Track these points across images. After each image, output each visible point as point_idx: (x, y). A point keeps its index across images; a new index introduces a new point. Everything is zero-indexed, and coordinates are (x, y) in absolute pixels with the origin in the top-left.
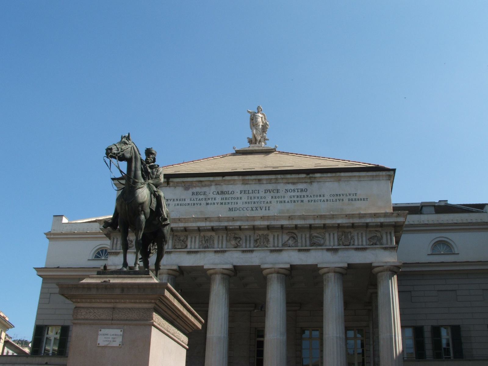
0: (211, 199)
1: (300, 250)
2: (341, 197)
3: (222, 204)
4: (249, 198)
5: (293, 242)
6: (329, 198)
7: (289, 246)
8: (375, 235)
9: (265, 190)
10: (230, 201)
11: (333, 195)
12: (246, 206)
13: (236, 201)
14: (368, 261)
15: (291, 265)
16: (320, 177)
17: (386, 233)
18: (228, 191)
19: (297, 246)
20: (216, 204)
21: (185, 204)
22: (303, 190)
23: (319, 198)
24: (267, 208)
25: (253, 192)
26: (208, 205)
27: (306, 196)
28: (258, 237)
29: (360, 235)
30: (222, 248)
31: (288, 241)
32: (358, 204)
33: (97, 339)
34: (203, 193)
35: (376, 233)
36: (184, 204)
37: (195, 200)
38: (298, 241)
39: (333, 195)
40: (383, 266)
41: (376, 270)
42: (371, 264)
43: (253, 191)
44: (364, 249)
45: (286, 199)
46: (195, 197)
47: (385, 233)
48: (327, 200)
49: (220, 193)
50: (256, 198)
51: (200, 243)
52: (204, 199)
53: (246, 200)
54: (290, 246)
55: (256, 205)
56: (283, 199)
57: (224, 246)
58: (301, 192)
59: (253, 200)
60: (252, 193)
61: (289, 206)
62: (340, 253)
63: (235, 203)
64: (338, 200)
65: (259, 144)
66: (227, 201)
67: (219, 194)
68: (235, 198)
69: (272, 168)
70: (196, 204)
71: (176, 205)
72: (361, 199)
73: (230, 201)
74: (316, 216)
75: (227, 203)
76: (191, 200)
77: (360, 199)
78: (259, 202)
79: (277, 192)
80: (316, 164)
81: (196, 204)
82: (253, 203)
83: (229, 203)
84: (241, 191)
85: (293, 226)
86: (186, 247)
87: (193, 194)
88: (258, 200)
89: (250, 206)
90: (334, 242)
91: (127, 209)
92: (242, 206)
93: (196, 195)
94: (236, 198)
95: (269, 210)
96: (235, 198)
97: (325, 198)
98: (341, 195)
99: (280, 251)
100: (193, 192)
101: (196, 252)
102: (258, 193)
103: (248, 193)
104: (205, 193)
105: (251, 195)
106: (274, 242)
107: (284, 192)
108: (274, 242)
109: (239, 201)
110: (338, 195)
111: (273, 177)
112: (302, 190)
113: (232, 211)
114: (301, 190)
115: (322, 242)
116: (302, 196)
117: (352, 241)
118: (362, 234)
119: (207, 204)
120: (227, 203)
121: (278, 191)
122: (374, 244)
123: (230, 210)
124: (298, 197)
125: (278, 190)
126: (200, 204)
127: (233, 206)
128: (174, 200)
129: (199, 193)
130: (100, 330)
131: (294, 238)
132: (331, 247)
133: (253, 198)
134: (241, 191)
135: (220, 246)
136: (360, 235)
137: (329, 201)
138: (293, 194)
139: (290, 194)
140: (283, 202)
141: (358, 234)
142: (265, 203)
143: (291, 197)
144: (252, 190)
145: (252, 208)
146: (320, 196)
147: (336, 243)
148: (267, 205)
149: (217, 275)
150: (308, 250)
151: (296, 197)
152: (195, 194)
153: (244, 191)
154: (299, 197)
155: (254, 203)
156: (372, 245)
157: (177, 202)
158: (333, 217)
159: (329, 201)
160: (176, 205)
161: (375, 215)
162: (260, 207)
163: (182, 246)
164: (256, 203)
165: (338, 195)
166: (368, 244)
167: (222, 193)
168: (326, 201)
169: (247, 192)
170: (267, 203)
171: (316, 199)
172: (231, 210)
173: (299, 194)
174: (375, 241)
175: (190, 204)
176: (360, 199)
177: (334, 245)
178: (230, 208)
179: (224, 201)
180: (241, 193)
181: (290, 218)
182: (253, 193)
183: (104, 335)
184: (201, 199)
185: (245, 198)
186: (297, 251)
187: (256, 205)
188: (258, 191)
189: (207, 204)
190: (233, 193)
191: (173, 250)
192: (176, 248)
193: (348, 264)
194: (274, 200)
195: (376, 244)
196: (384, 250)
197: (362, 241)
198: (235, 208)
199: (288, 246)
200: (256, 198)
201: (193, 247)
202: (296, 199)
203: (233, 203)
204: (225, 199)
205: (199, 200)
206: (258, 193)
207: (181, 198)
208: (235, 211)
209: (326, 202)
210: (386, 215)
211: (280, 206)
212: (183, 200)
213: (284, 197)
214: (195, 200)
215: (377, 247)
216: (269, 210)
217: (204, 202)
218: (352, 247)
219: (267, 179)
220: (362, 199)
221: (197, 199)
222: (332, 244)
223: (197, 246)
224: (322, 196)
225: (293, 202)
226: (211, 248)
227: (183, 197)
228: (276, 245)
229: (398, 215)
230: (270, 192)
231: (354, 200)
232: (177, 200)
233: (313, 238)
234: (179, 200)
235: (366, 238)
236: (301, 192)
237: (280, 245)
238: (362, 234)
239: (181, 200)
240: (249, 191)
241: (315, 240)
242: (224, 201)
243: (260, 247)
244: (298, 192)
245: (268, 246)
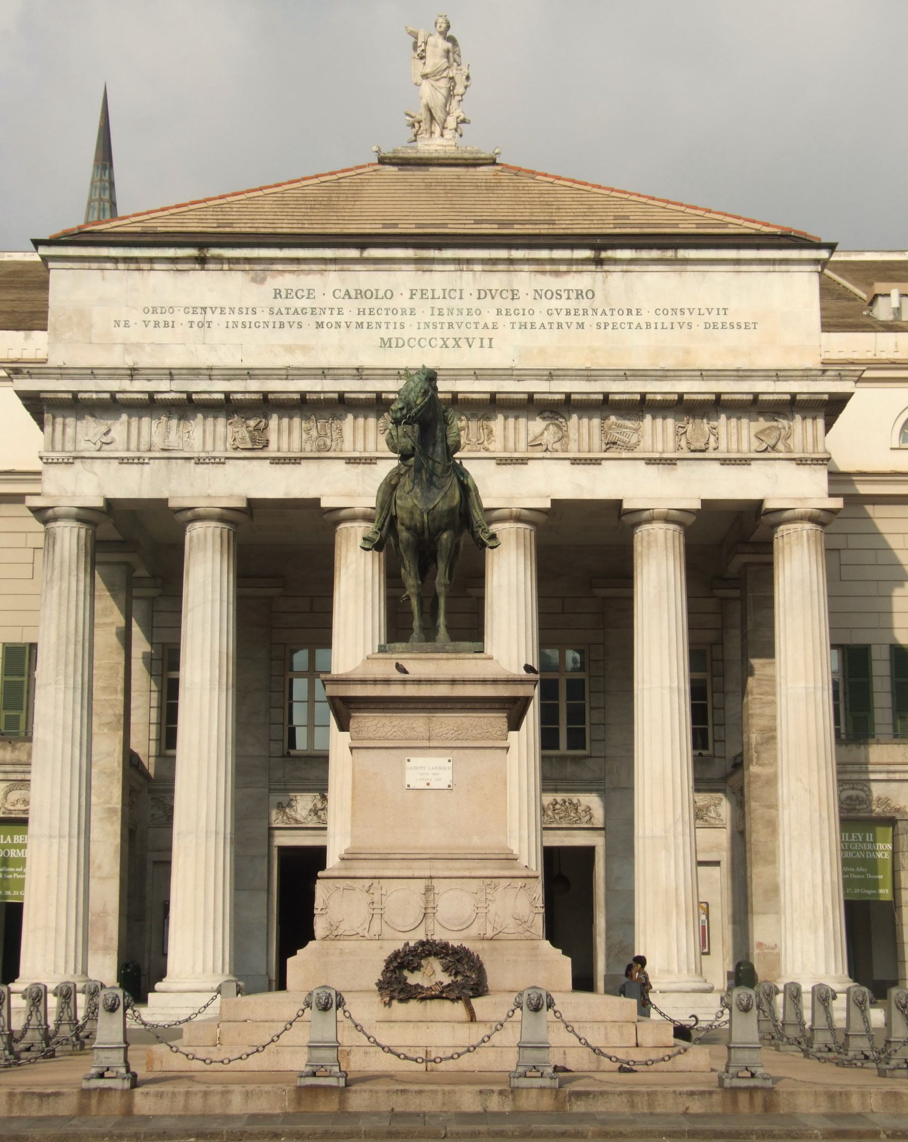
0: (328, 312)
1: (575, 461)
2: (687, 317)
3: (360, 325)
4: (436, 312)
5: (556, 439)
6: (653, 319)
7: (547, 450)
9: (479, 291)
10: (382, 318)
11: (665, 312)
12: (430, 333)
13: (398, 318)
14: (753, 495)
15: (553, 501)
16: (631, 261)
18: (377, 290)
19: (566, 451)
20: (343, 324)
21: (257, 324)
22: (584, 294)
23: (626, 318)
24: (486, 342)
25: (447, 294)
26: (320, 329)
27: (590, 312)
28: (464, 423)
30: (365, 450)
31: (542, 434)
32: (731, 337)
33: (404, 777)
34: (306, 293)
36: (253, 325)
37: (284, 311)
38: (568, 436)
39: (665, 312)
41: (772, 518)
42: (761, 502)
43: (447, 292)
44: (745, 462)
45: (538, 319)
46: (281, 303)
48: (648, 326)
49: (353, 294)
50: (455, 312)
51: (304, 436)
52: (309, 311)
53: (429, 319)
54: (550, 448)
55: (455, 332)
56: (527, 319)
57: (371, 446)
58: (577, 298)
59: (446, 319)
60: (444, 298)
61: (546, 338)
62: (682, 469)
63: (398, 326)
64: (676, 326)
65: (442, 135)
66: (375, 319)
67: (350, 298)
68: (394, 311)
69: (496, 226)
70: (287, 325)
71: (231, 325)
72: (739, 327)
73: (382, 318)
74: (622, 373)
75: (374, 325)
76: (271, 312)
77: (735, 326)
78: (464, 325)
79: (513, 299)
80: (616, 218)
81: (287, 325)
82: (446, 326)
83: (379, 325)
84: (412, 290)
85: (557, 397)
86: (266, 445)
87: (276, 293)
88: (460, 319)
89: (438, 333)
90: (664, 441)
91: (426, 520)
92: (418, 335)
93: (287, 297)
94: (400, 312)
95: (491, 347)
96: (394, 311)
97: (642, 319)
98: (687, 312)
99: (523, 461)
100: (276, 290)
101: (296, 461)
102: (461, 298)
103: (433, 298)
104: (310, 294)
105: (439, 303)
106: (505, 438)
107: (530, 298)
108: (505, 438)
109: (407, 319)
110: (679, 312)
111: (502, 254)
112: (579, 294)
113: (390, 347)
114: (578, 295)
115: (634, 440)
116: (581, 312)
117: (712, 439)
119: (320, 325)
120: (374, 325)
121: (514, 295)
122: (769, 449)
123: (386, 344)
124: (568, 313)
125: (515, 292)
126: (300, 326)
127: (393, 333)
128: (222, 312)
129: (294, 294)
130: (409, 761)
131: (559, 427)
132: (657, 455)
133: (445, 312)
134: (412, 290)
135: (360, 445)
137: (653, 326)
138: (555, 303)
139: (545, 304)
140: (529, 326)
142: (480, 326)
143: (549, 313)
144: (444, 290)
145: (445, 343)
146: (629, 311)
147: (671, 445)
148: (486, 334)
149: (355, 524)
150: (596, 462)
151: (564, 312)
152: (284, 295)
153: (422, 290)
154: (573, 312)
155: (451, 326)
156: (765, 450)
157: (231, 318)
158: (665, 375)
159: (653, 326)
160: (231, 325)
161: (778, 375)
162: (467, 339)
163: (253, 440)
164: (455, 326)
165: (679, 312)
166: (753, 448)
167: (361, 294)
168: (644, 326)
169: (430, 294)
170: (486, 326)
171: (617, 319)
172: (388, 345)
173: (572, 304)
174: (772, 442)
175: (271, 325)
176: (735, 326)
178: (382, 339)
179: (365, 319)
180: (411, 298)
181: (551, 375)
182: (447, 296)
183: (416, 768)
184: (299, 311)
185: (423, 308)
186: (568, 462)
187: (455, 332)
188: (458, 292)
189: (320, 325)
190: (389, 294)
191: (228, 455)
192: (236, 449)
193: (704, 502)
194: (504, 320)
195: (774, 448)
197: (739, 440)
198: (397, 339)
199: (544, 447)
200: (455, 312)
201: (285, 446)
202: (563, 318)
203: (391, 326)
204: (367, 312)
205: (296, 311)
206: (461, 298)
207: (244, 305)
208: (397, 346)
209: (644, 331)
210: (806, 374)
211: (520, 338)
212: (250, 311)
213: (531, 312)
214: (284, 311)
215: (779, 459)
216: (491, 347)
217: (308, 320)
218: (713, 456)
219: (484, 261)
220: (743, 326)
221: (288, 309)
222: (660, 448)
223: (296, 446)
224: (634, 312)
225: (555, 326)
226: (335, 450)
227: (250, 302)
228: (511, 445)
229: (840, 377)
230: (493, 298)
231: (720, 325)
232: (232, 310)
233: (610, 428)
234: (236, 311)
236: (577, 298)
237: (522, 445)
239: (244, 311)
240: (433, 291)
241: (615, 435)
242: (365, 319)
243: (469, 451)
244: (569, 298)
245: (491, 447)
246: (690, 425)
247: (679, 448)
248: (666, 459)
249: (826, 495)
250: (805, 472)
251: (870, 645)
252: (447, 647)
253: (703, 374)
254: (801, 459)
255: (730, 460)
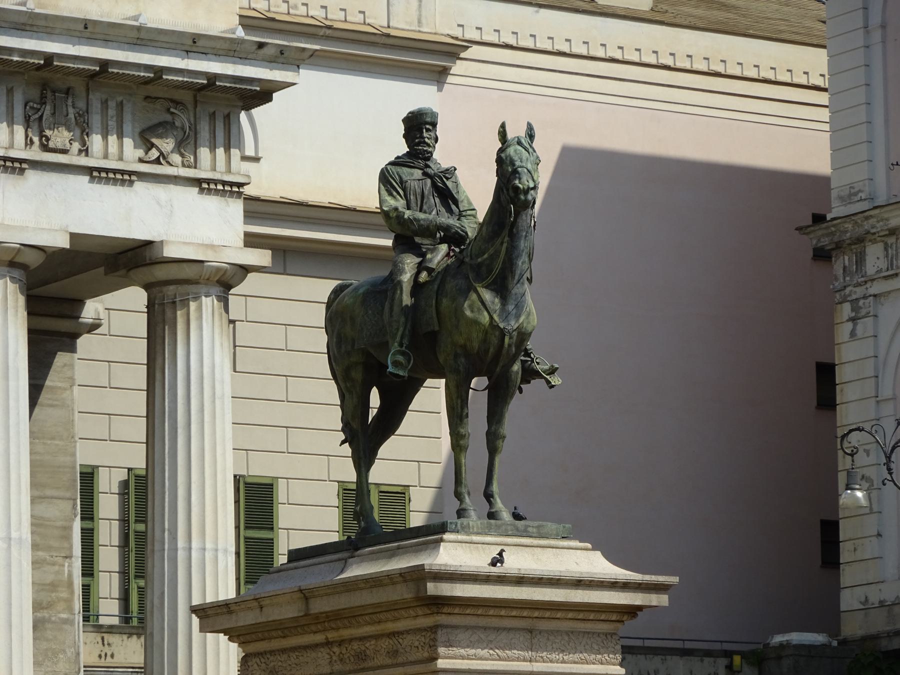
8: (168, 118)
17: (213, 116)
29: (112, 112)
35: (173, 113)
40: (202, 262)
42: (149, 243)
47: (208, 118)
118: (120, 106)
136: (112, 112)
141: (105, 104)
156: (157, 161)
161: (193, 44)
177: (11, 146)
193: (74, 236)
196: (202, 190)
218: (83, 161)
235: (133, 127)
238: (120, 106)
246: (48, 107)
247: (29, 143)
248: (13, 160)
249: (242, 244)
250: (212, 203)
251: (98, 467)
252: (530, 529)
253: (87, 30)
254: (208, 181)
255: (107, 171)
